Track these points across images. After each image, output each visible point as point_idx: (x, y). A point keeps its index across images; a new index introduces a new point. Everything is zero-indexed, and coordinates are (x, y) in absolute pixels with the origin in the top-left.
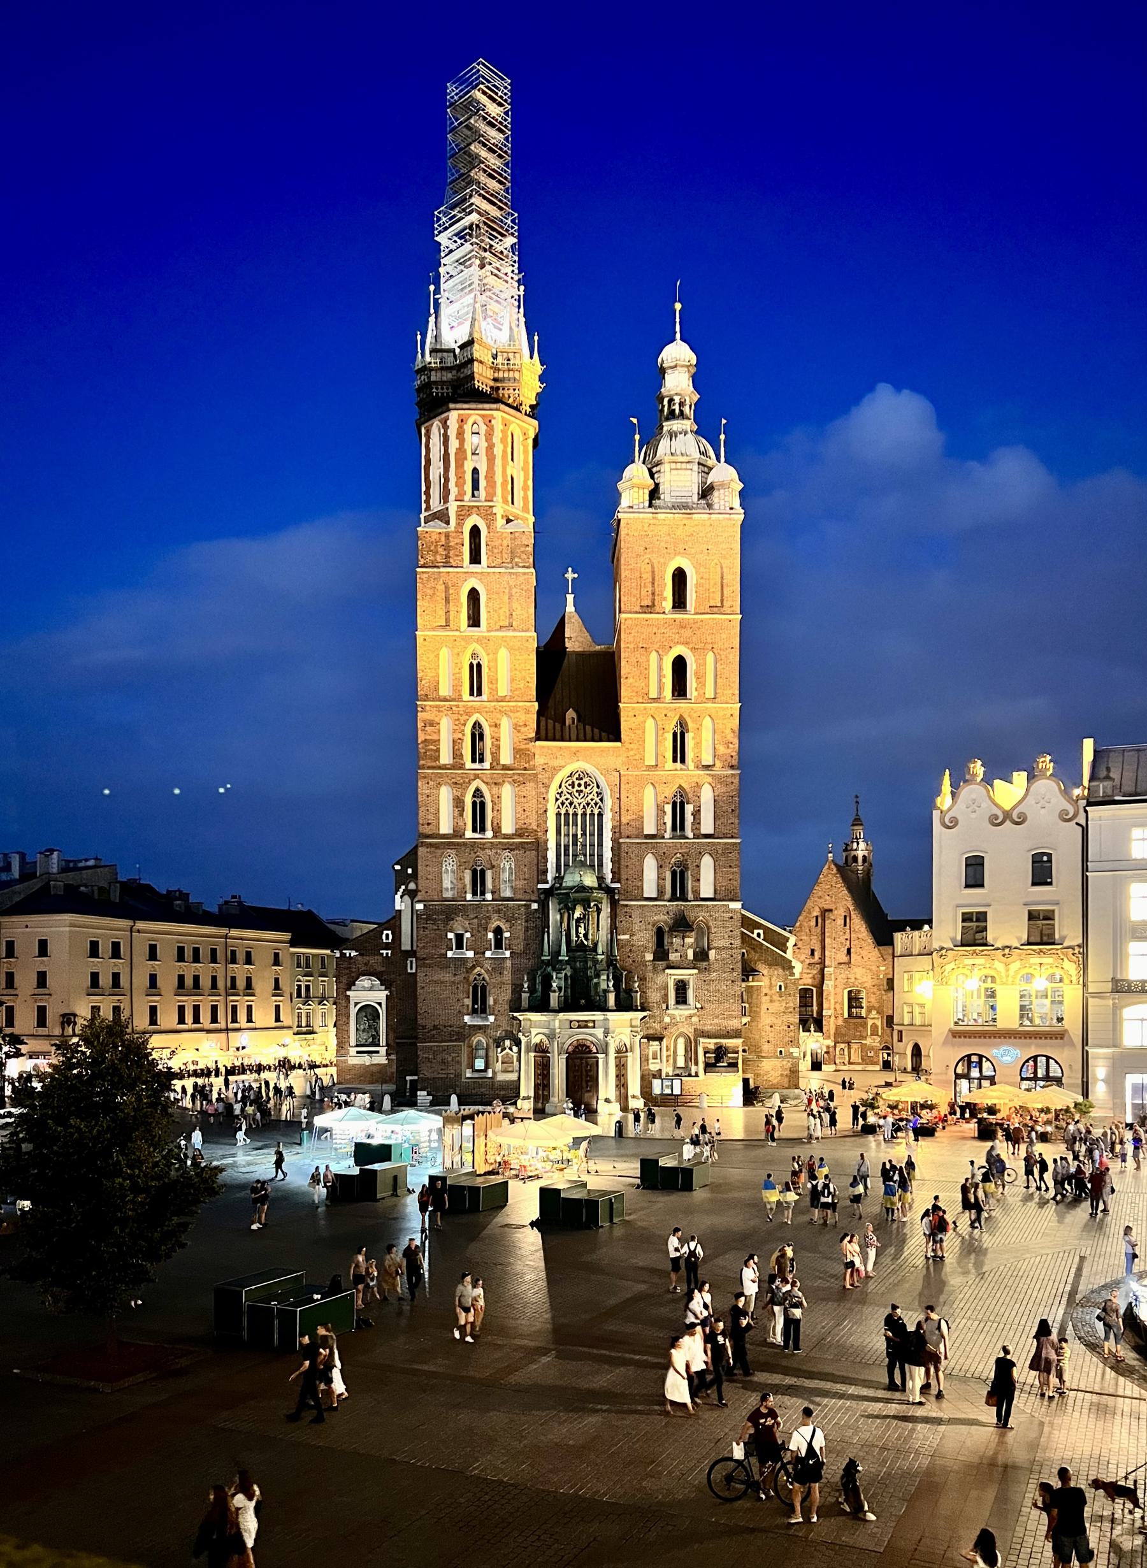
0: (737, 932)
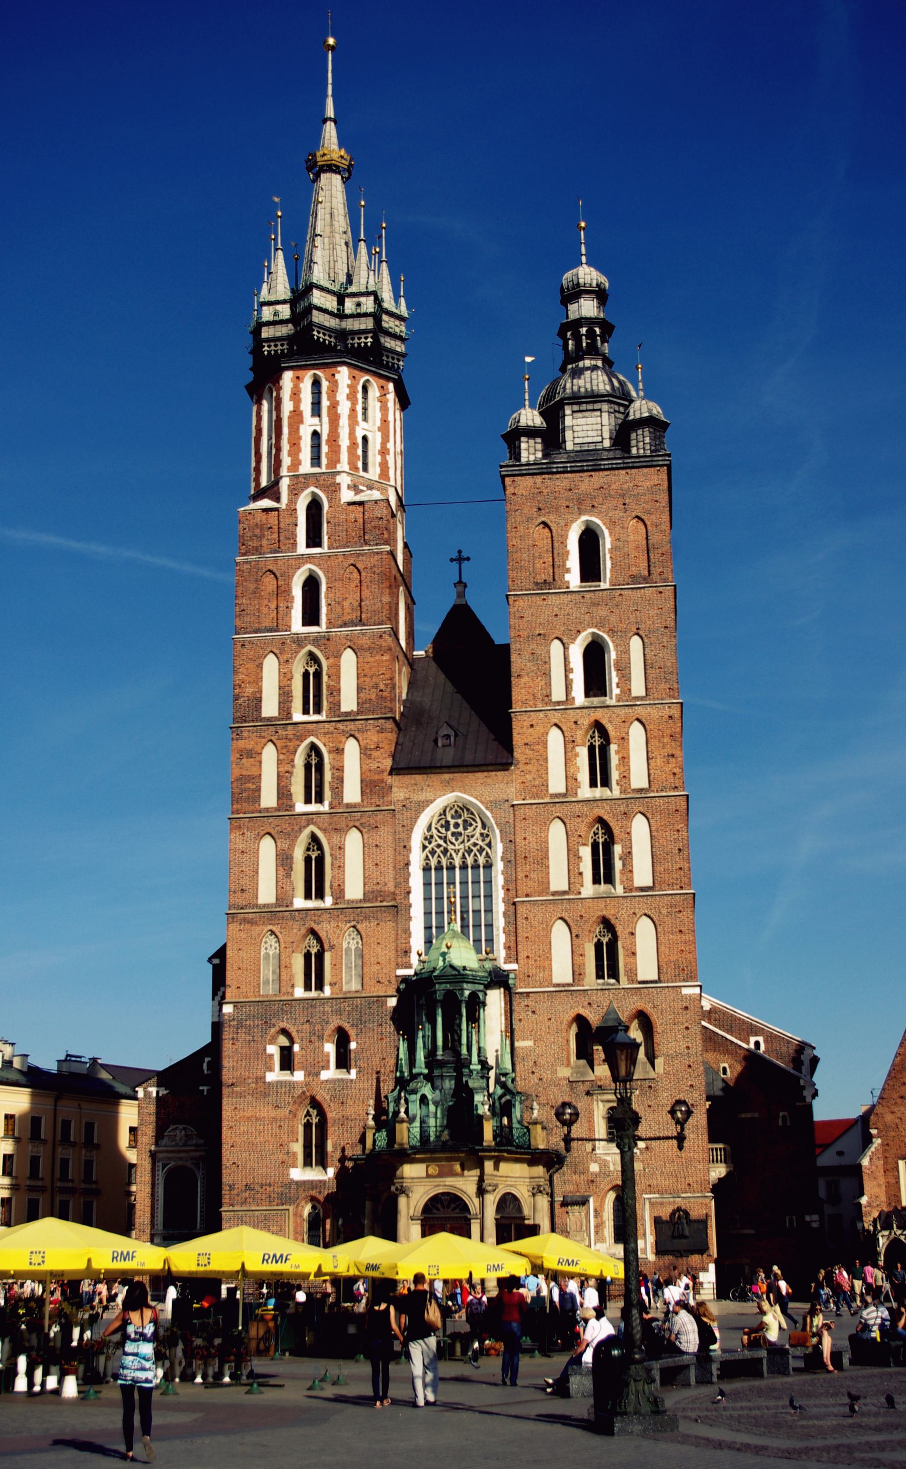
0: (698, 1029)
